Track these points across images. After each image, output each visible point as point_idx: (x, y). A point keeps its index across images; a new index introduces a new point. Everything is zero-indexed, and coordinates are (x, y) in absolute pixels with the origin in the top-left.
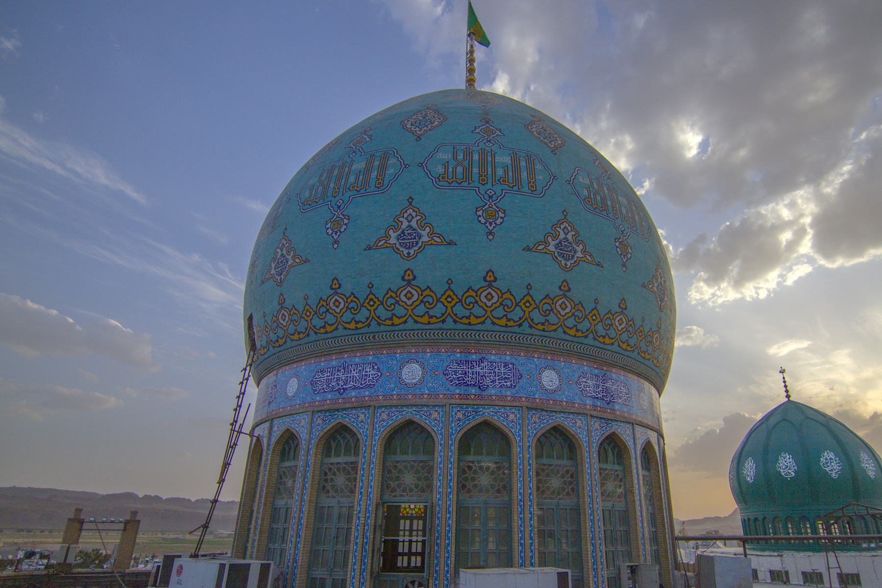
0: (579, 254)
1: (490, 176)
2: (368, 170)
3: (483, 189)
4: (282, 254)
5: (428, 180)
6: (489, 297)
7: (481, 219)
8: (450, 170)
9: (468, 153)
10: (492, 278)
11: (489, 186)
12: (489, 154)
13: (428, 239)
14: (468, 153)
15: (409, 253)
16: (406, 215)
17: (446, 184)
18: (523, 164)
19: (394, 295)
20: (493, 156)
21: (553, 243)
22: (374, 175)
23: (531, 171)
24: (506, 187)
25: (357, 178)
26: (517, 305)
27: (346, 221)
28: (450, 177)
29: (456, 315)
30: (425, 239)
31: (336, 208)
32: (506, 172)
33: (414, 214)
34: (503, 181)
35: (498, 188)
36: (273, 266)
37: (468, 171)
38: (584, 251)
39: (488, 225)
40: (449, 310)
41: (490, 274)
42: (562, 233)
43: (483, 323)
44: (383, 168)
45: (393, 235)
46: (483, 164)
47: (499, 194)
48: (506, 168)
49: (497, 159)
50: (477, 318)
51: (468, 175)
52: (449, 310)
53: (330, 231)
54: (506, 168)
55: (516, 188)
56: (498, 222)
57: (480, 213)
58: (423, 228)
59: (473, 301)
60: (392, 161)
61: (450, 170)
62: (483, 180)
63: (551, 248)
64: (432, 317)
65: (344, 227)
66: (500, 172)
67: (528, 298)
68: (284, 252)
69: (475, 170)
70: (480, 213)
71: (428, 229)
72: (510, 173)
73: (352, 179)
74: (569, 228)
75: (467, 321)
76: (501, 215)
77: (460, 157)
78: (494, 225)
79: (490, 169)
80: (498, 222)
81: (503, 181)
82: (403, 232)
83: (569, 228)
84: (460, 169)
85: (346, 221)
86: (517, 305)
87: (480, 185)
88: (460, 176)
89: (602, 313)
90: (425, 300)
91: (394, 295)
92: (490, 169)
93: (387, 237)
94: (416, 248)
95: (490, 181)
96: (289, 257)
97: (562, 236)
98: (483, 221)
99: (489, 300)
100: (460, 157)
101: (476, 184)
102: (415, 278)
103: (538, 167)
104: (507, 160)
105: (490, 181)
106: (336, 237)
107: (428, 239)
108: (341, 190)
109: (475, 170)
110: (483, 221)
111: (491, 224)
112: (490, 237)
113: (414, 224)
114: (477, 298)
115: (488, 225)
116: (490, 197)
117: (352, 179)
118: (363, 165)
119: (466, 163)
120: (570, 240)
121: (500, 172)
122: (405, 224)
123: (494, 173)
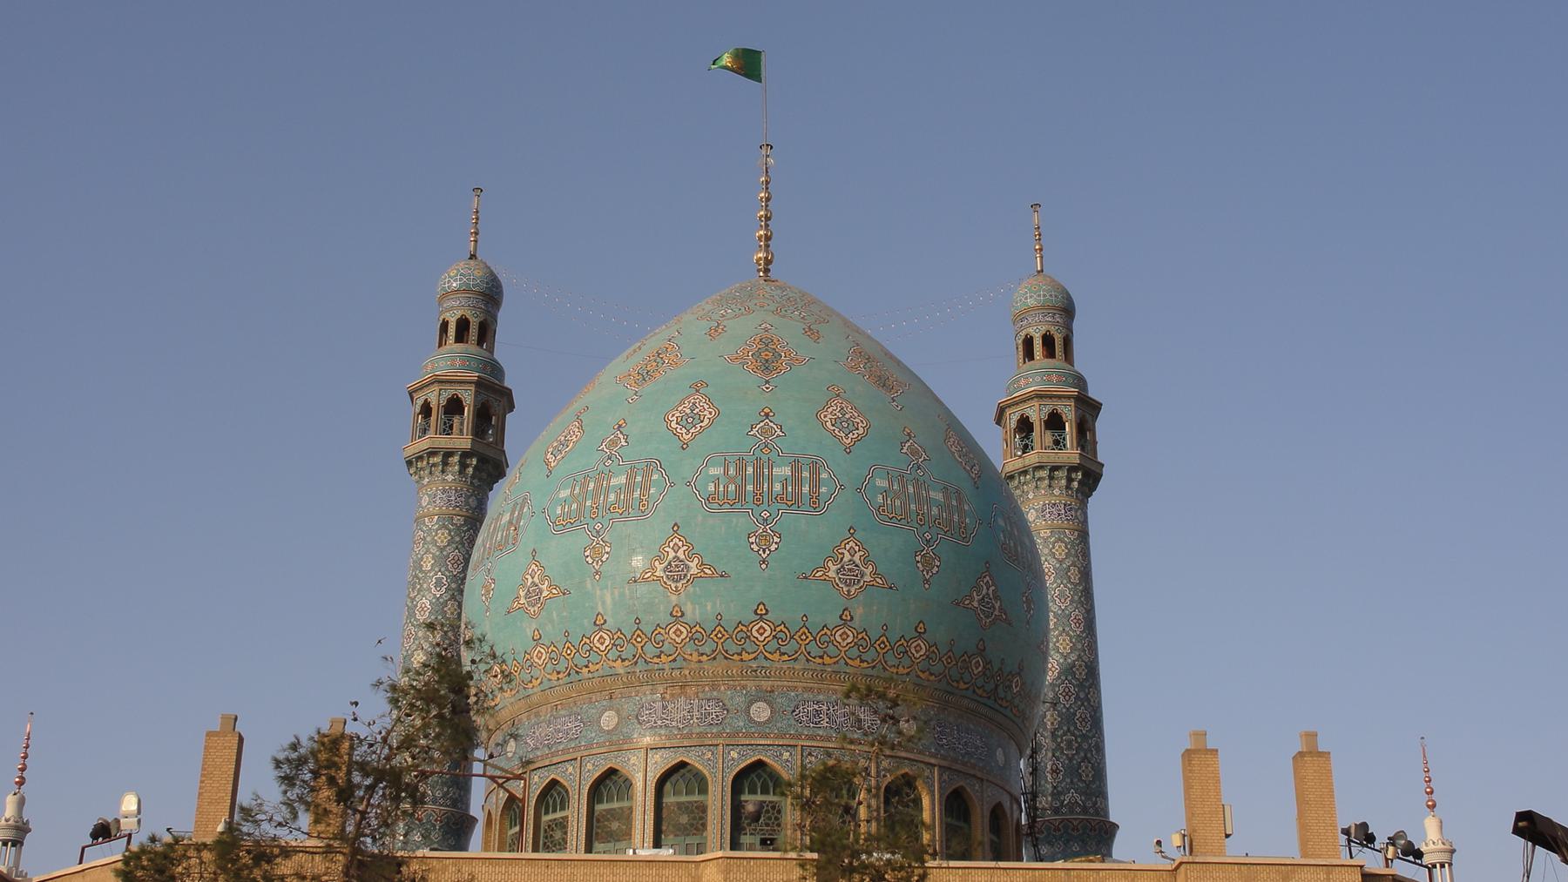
0: (868, 578)
2: (630, 486)
6: (761, 631)
9: (741, 468)
11: (765, 506)
14: (741, 468)
18: (806, 474)
20: (771, 468)
21: (834, 568)
23: (816, 483)
30: (694, 570)
32: (784, 487)
34: (780, 498)
37: (741, 491)
45: (660, 567)
46: (758, 476)
51: (741, 494)
56: (773, 547)
58: (690, 558)
62: (758, 499)
63: (832, 574)
66: (777, 487)
69: (750, 488)
77: (732, 472)
80: (773, 547)
84: (732, 487)
88: (731, 496)
93: (653, 569)
97: (847, 557)
100: (732, 472)
103: (824, 476)
104: (787, 471)
109: (750, 488)
113: (681, 555)
118: (622, 479)
121: (777, 487)
122: (672, 554)
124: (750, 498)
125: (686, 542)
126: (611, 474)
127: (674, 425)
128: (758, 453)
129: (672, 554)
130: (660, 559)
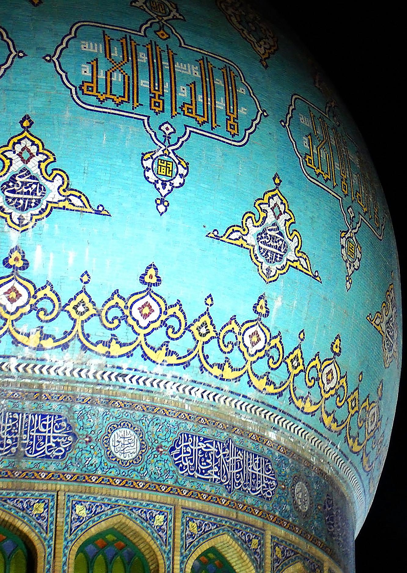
3: (156, 121)
5: (63, 88)
7: (149, 174)
8: (102, 76)
10: (154, 280)
12: (164, 54)
13: (58, 198)
17: (93, 100)
19: (122, 304)
20: (172, 62)
24: (193, 123)
26: (188, 328)
28: (102, 89)
29: (87, 337)
35: (181, 120)
38: (299, 249)
40: (78, 327)
41: (152, 271)
42: (270, 213)
43: (129, 355)
47: (179, 134)
50: (122, 345)
52: (78, 327)
55: (207, 127)
56: (177, 181)
59: (120, 314)
61: (102, 76)
64: (47, 337)
67: (206, 318)
74: (282, 207)
75: (105, 349)
76: (182, 171)
78: (168, 187)
79: (167, 85)
80: (177, 181)
81: (187, 109)
83: (282, 207)
86: (188, 328)
87: (151, 113)
88: (118, 90)
89: (307, 359)
90: (39, 306)
91: (122, 304)
92: (167, 85)
94: (36, 211)
95: (167, 107)
98: (152, 178)
99: (146, 316)
105: (167, 107)
107: (58, 198)
110: (152, 178)
111: (164, 185)
112: (162, 208)
114: (127, 312)
115: (159, 185)
116: (167, 137)
120: (282, 228)
121: (183, 93)
123: (174, 91)
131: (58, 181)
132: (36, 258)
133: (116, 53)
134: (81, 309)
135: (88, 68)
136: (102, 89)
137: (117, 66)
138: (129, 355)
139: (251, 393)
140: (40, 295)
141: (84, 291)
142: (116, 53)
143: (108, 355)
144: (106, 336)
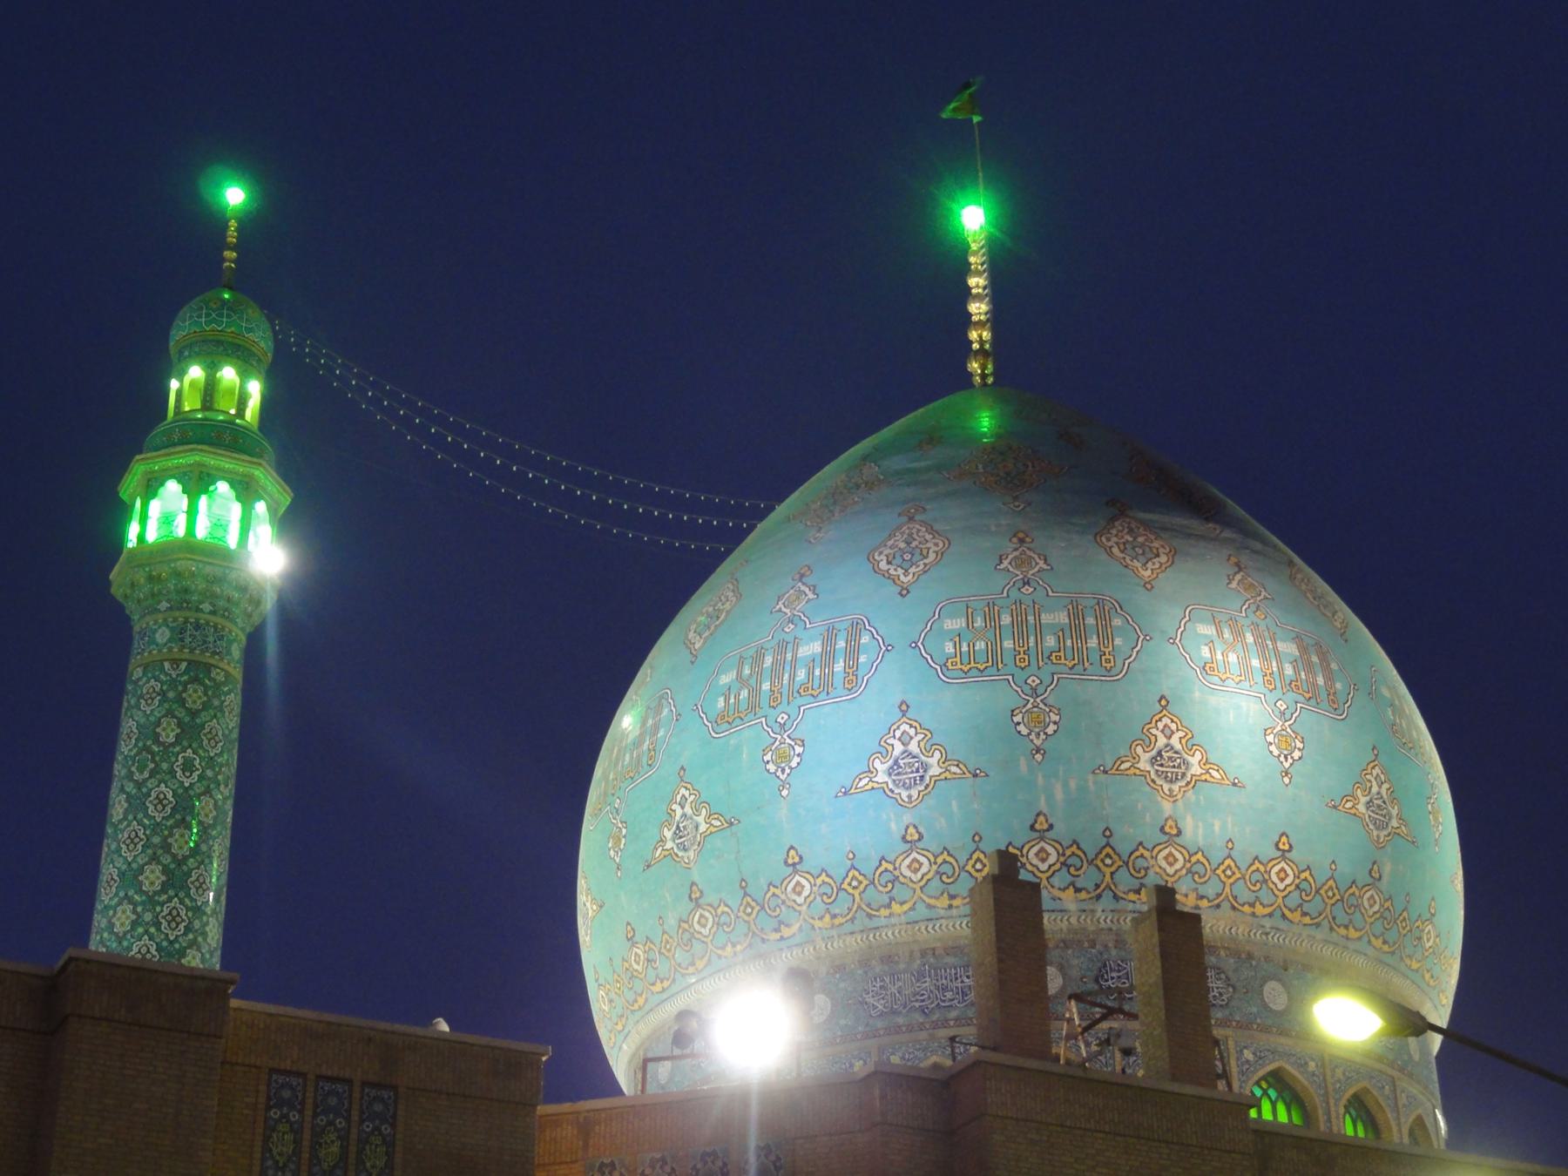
1: (1033, 652)
2: (828, 656)
4: (684, 815)
7: (1021, 728)
8: (965, 648)
12: (1030, 611)
15: (910, 797)
16: (898, 734)
22: (839, 667)
25: (810, 673)
27: (799, 750)
31: (777, 729)
33: (912, 732)
36: (668, 834)
39: (1033, 736)
44: (853, 652)
48: (1060, 633)
49: (1046, 618)
53: (772, 767)
54: (1060, 633)
56: (1050, 730)
57: (1018, 719)
60: (865, 639)
65: (797, 760)
66: (1050, 642)
68: (688, 810)
70: (1018, 719)
71: (937, 755)
72: (1069, 643)
73: (801, 675)
78: (1043, 736)
79: (1032, 639)
80: (1050, 730)
82: (896, 762)
85: (799, 750)
87: (1017, 671)
92: (1032, 639)
96: (701, 819)
100: (979, 623)
101: (1011, 668)
102: (921, 838)
104: (1062, 618)
106: (783, 777)
108: (785, 692)
110: (1025, 731)
116: (1034, 690)
117: (801, 675)
118: (816, 647)
119: (990, 635)
121: (1050, 642)
122: (899, 748)
124: (1008, 659)
125: (918, 726)
126: (796, 643)
127: (883, 565)
128: (1014, 594)
129: (899, 748)
130: (884, 752)
131: (937, 755)
132: (1188, 825)
133: (1227, 635)
134: (1229, 873)
135: (951, 645)
136: (965, 660)
137: (1231, 647)
138: (1270, 915)
139: (1371, 951)
140: (1194, 859)
141: (853, 867)
142: (1227, 635)
143: (1253, 914)
144: (1250, 897)
